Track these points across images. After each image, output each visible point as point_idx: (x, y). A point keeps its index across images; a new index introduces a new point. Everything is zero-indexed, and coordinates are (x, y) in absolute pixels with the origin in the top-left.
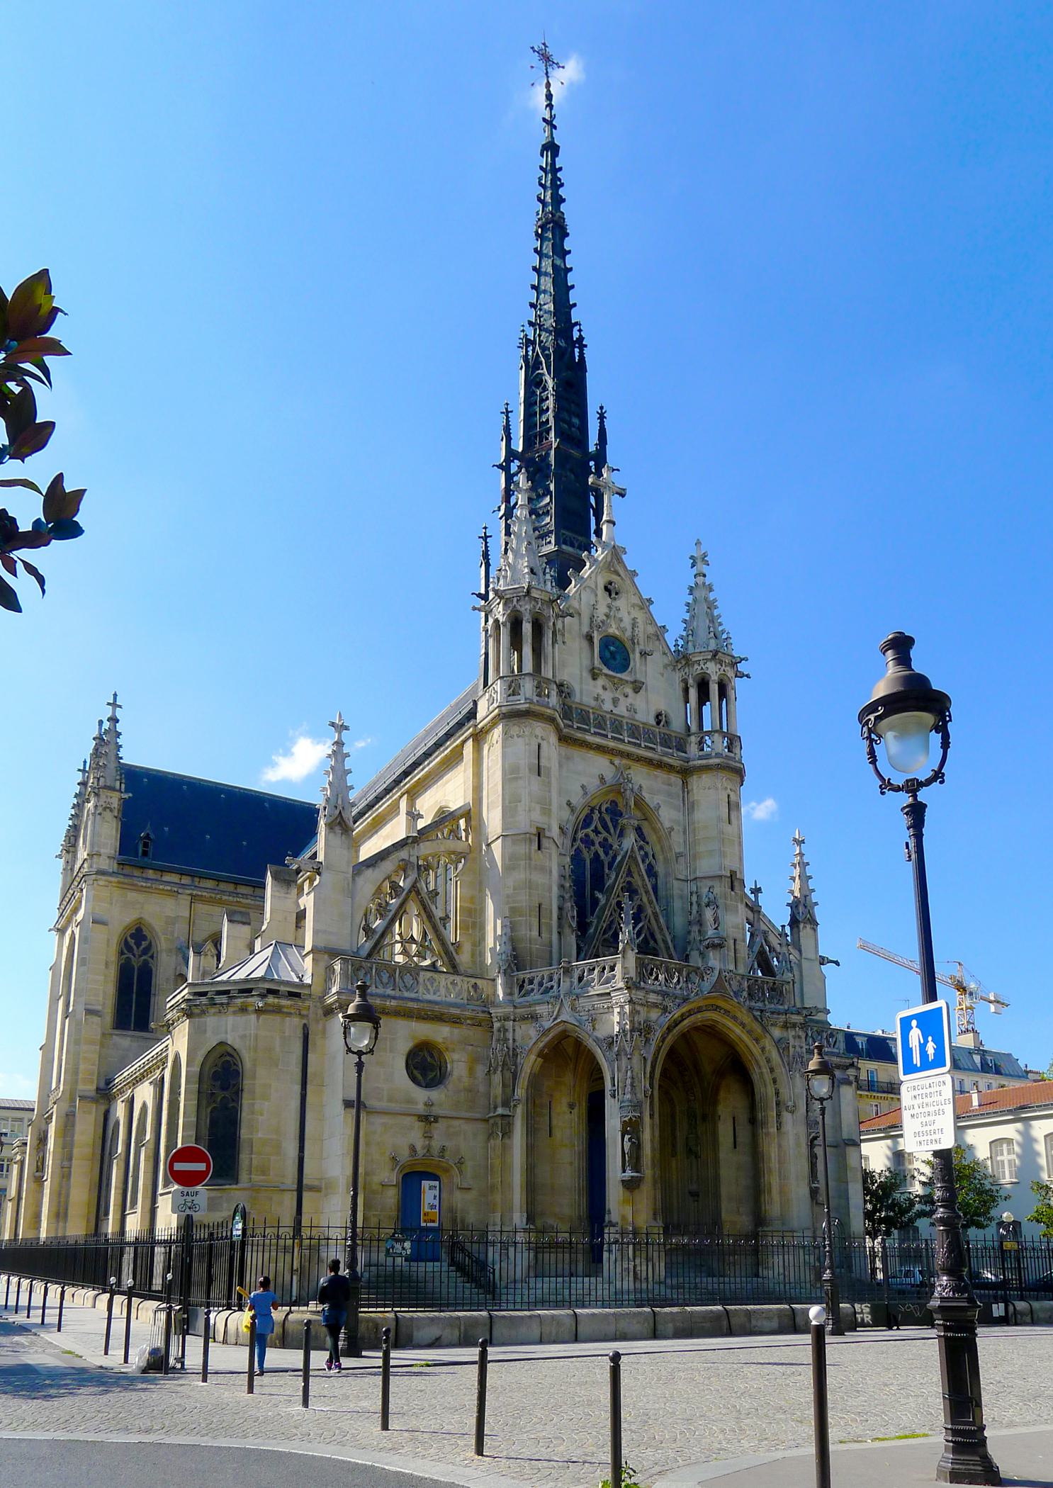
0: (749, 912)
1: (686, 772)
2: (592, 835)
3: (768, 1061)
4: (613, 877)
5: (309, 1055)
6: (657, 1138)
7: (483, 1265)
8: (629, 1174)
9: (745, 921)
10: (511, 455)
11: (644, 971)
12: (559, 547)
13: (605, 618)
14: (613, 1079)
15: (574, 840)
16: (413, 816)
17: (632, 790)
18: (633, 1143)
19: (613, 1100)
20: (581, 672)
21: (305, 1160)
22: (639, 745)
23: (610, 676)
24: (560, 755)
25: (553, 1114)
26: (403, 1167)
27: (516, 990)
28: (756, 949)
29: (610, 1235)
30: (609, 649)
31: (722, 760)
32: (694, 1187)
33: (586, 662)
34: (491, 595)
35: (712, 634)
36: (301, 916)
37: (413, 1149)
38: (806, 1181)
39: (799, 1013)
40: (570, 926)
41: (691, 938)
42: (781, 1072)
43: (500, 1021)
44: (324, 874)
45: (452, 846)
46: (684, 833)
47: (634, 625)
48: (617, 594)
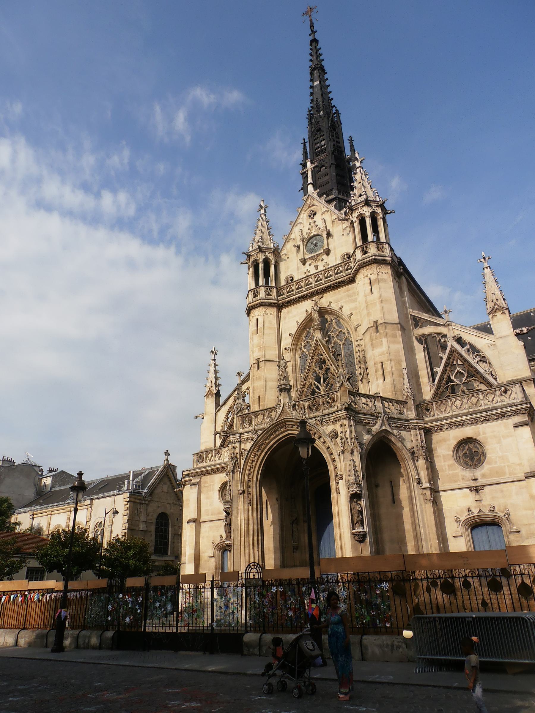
3: (328, 448)
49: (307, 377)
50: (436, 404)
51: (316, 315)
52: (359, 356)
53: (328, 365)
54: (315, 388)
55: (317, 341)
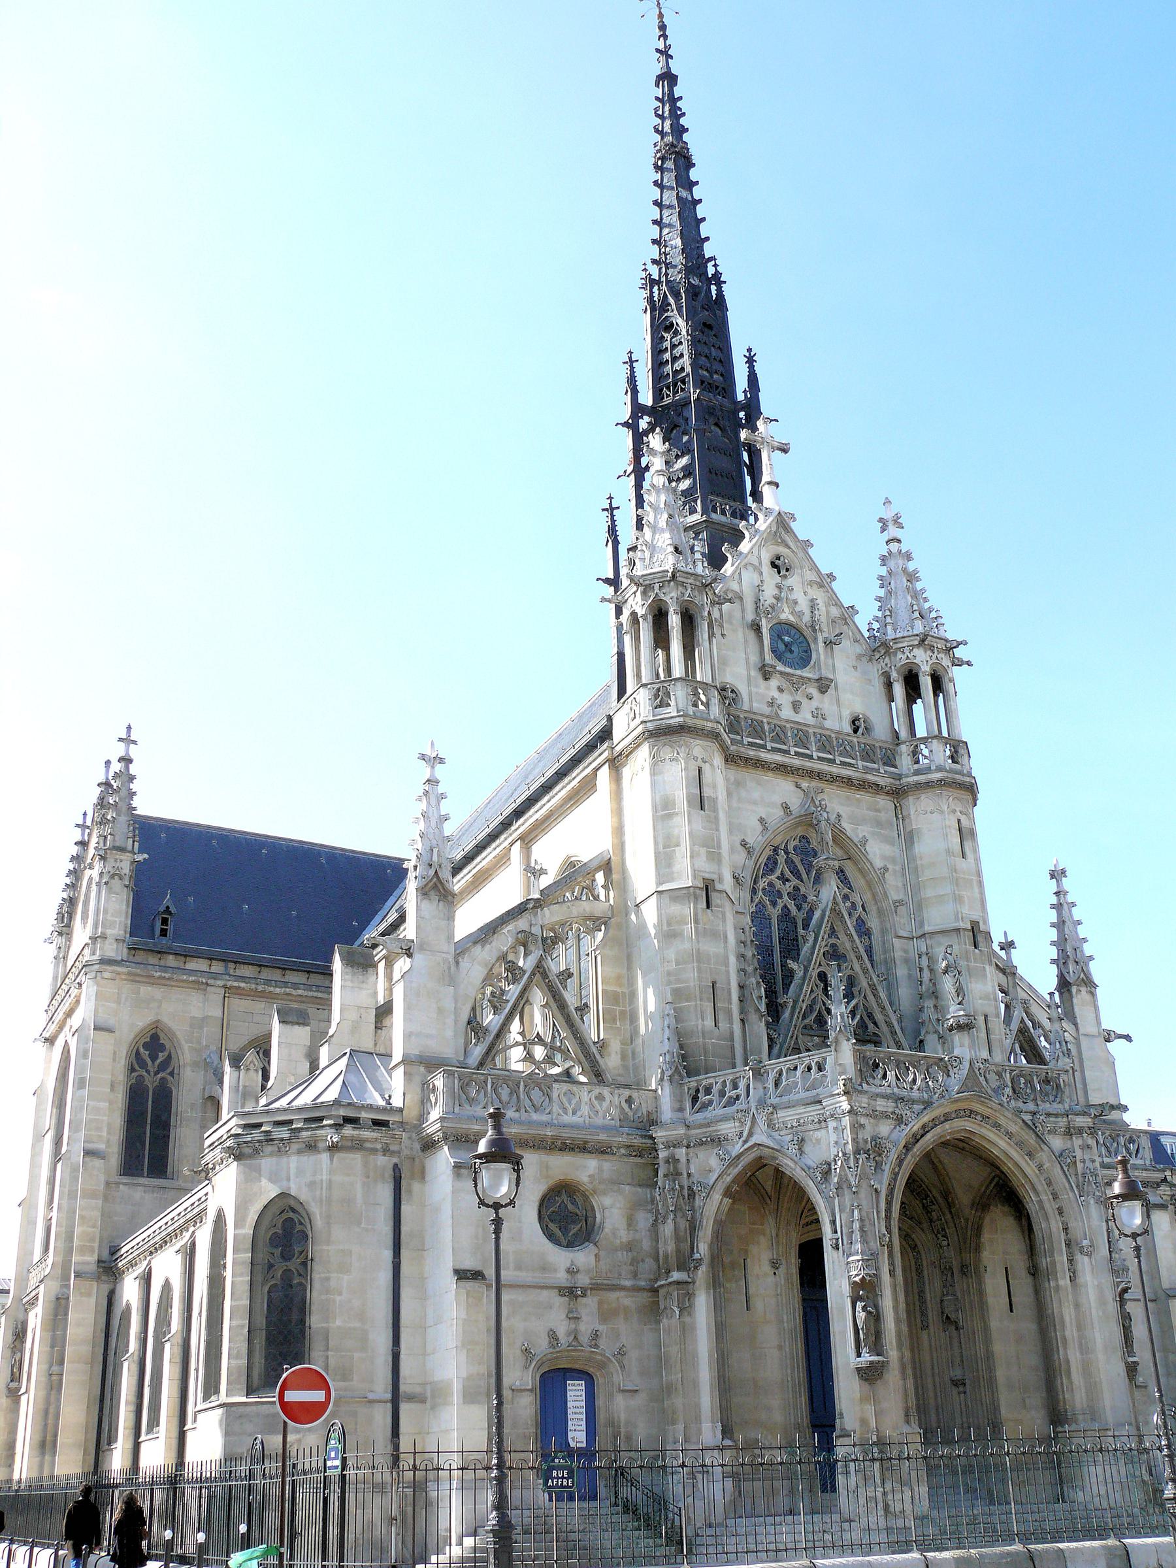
0: (1001, 975)
1: (898, 793)
2: (778, 884)
4: (811, 939)
5: (404, 1208)
6: (902, 1306)
7: (660, 1502)
8: (867, 1358)
9: (997, 988)
10: (638, 410)
11: (869, 1068)
12: (708, 516)
13: (774, 601)
14: (833, 1222)
15: (754, 891)
16: (533, 872)
17: (828, 820)
18: (869, 1313)
19: (835, 1253)
20: (748, 670)
21: (402, 1357)
22: (833, 761)
23: (788, 674)
24: (727, 780)
25: (750, 1278)
26: (541, 1364)
27: (688, 1104)
28: (1015, 1026)
29: (841, 1450)
30: (782, 640)
31: (946, 774)
32: (957, 1373)
33: (754, 658)
34: (625, 582)
35: (917, 614)
36: (384, 1011)
37: (553, 1336)
38: (1119, 1353)
39: (1084, 1114)
40: (758, 1010)
41: (925, 1016)
42: (1068, 1197)
43: (667, 1147)
44: (417, 956)
45: (588, 909)
46: (904, 875)
47: (813, 606)
48: (787, 570)
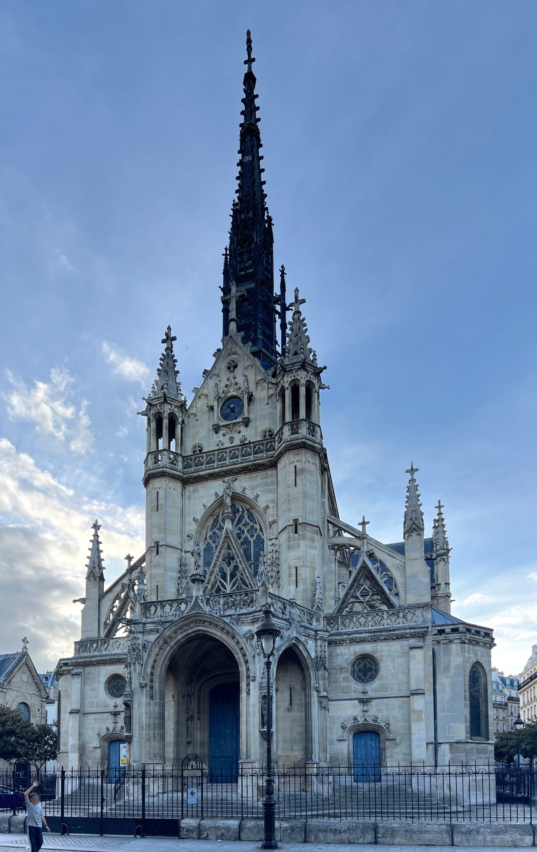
49: (213, 572)
50: (341, 618)
51: (228, 501)
52: (272, 557)
53: (237, 562)
54: (220, 586)
55: (227, 533)
